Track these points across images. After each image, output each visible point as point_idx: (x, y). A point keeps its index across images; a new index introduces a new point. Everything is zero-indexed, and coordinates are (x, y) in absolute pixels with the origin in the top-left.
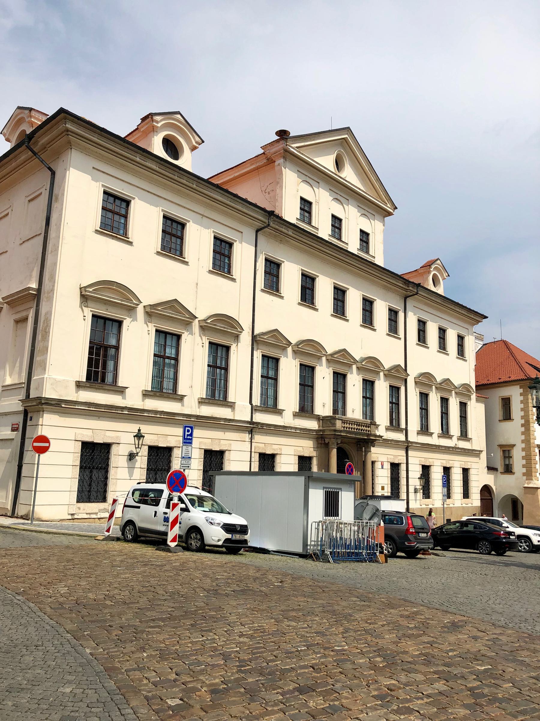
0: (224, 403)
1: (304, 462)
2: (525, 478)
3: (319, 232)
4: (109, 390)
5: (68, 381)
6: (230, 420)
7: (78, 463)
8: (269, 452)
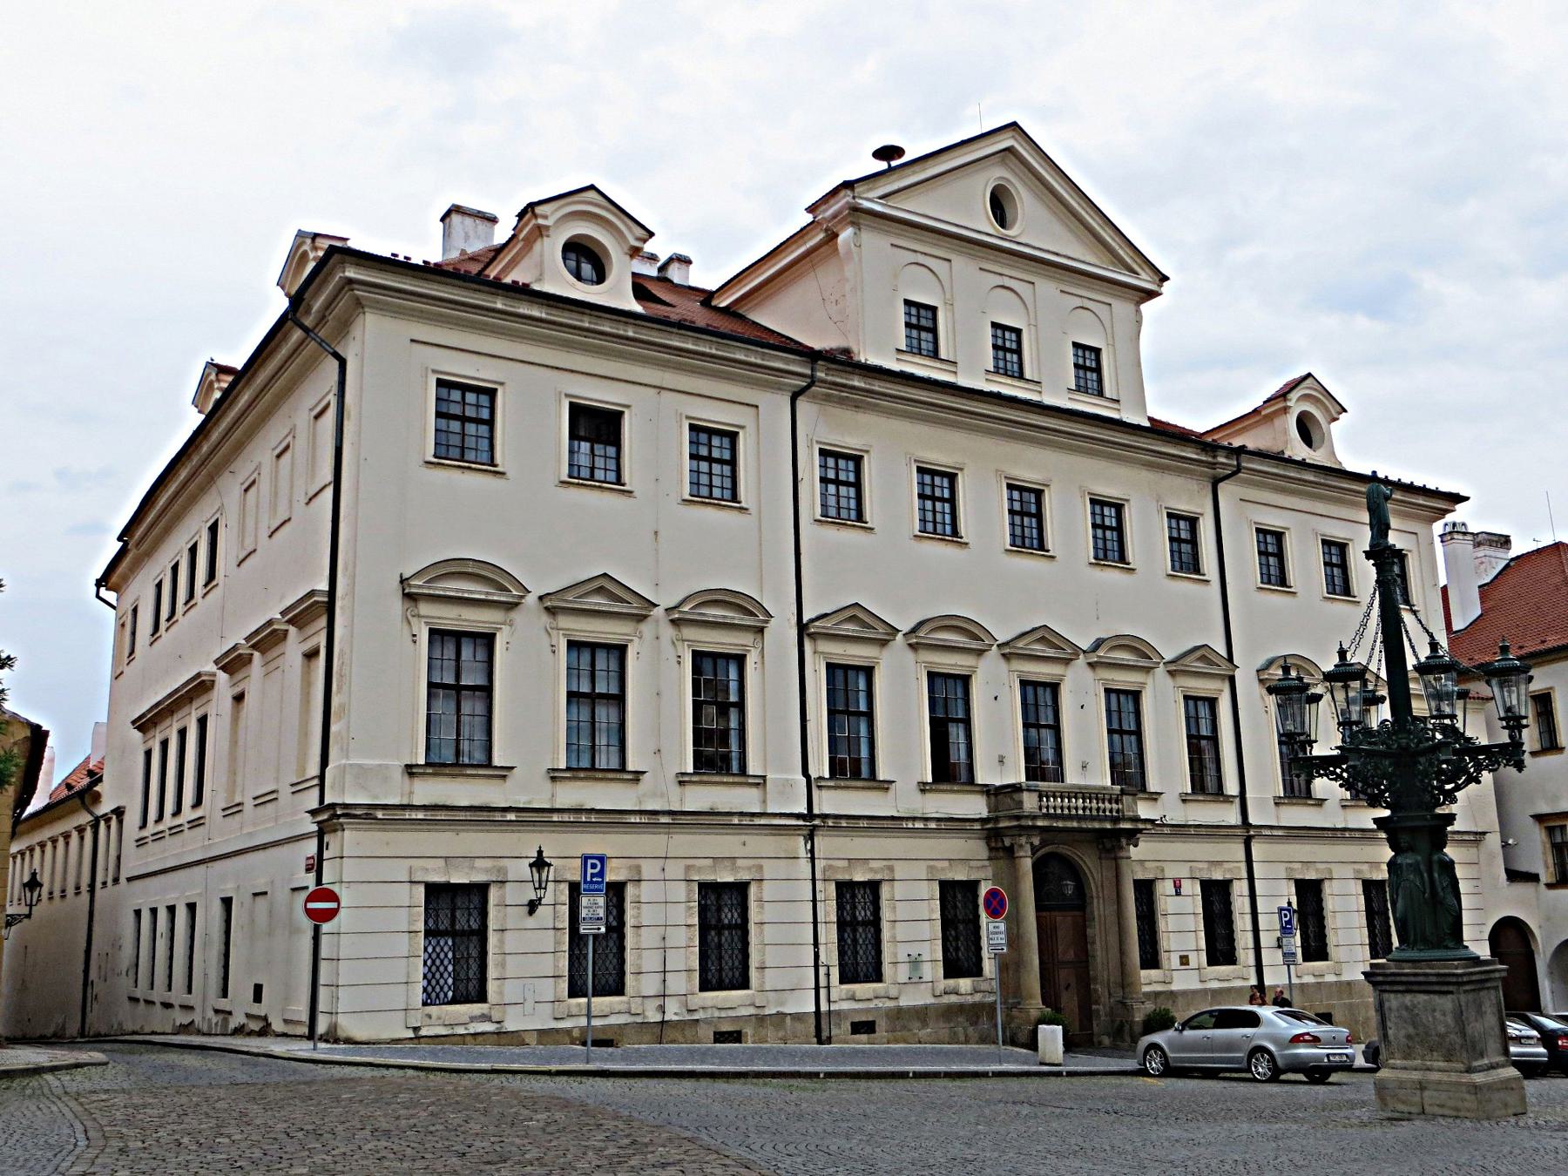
0: (737, 779)
3: (960, 369)
5: (387, 767)
6: (753, 815)
8: (859, 877)
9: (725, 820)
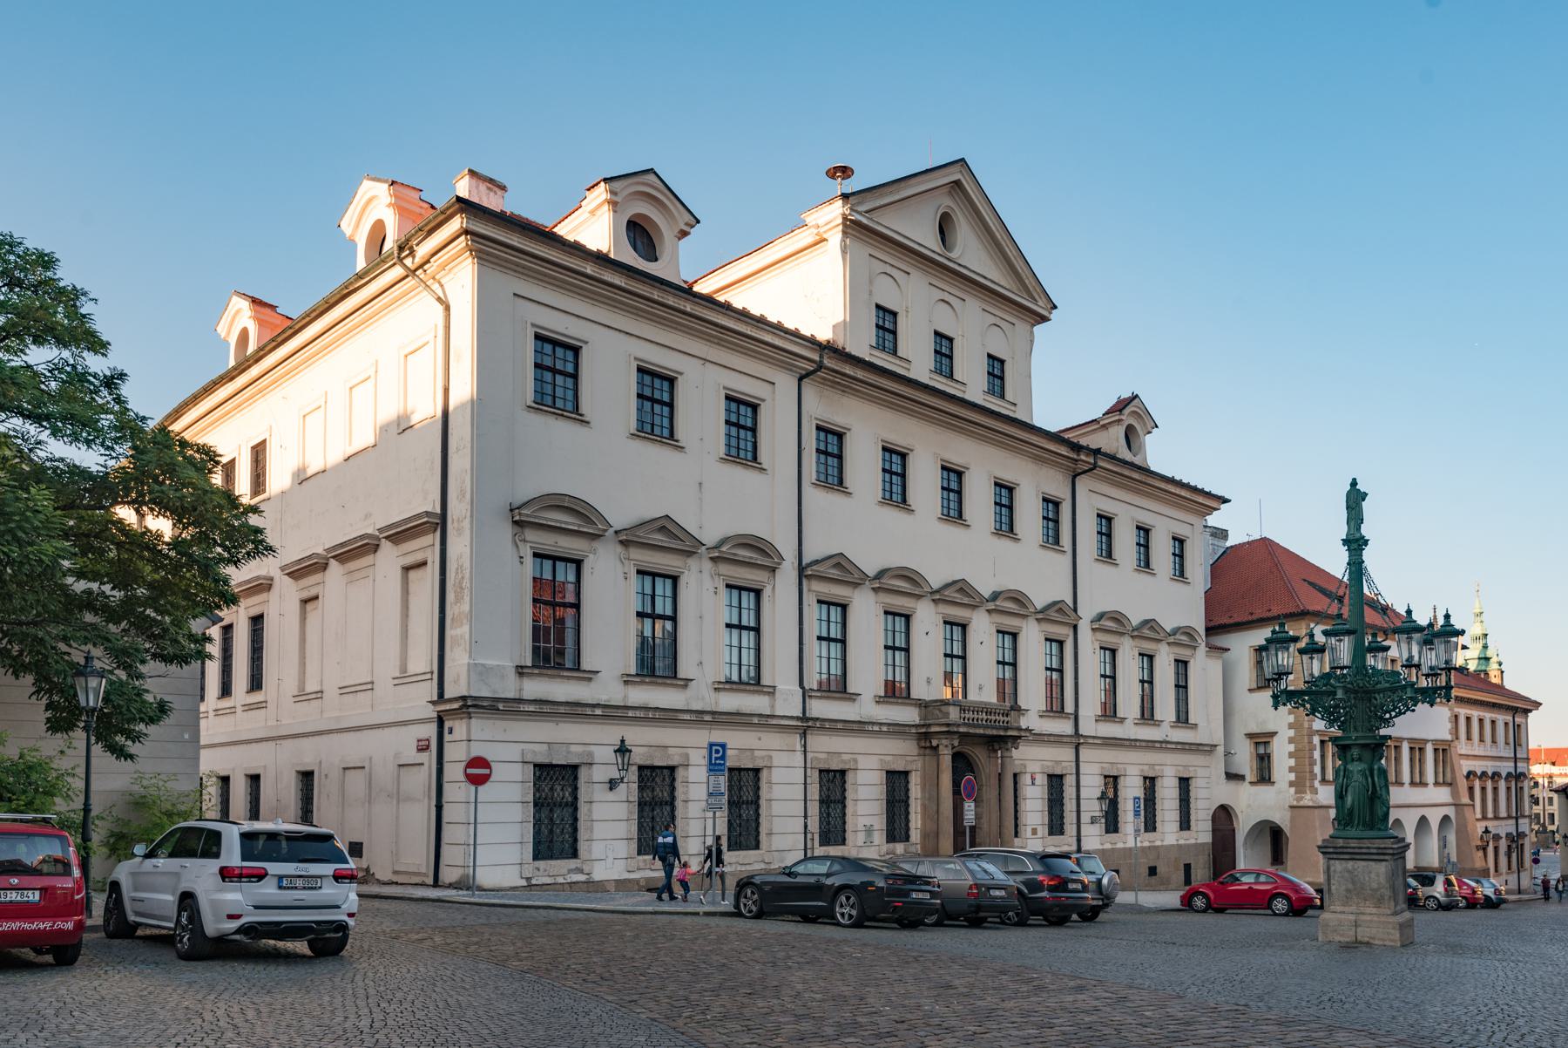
1: (896, 781)
2: (1293, 790)
4: (568, 678)
7: (530, 798)
8: (834, 767)
9: (579, 710)
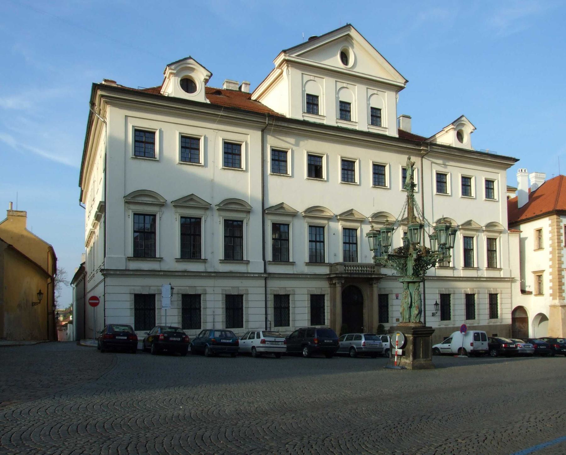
2: (551, 298)
8: (282, 293)
